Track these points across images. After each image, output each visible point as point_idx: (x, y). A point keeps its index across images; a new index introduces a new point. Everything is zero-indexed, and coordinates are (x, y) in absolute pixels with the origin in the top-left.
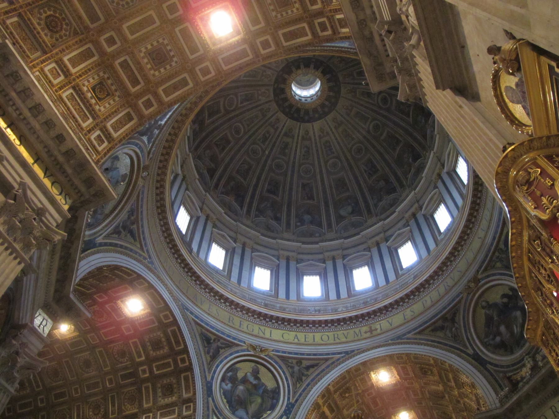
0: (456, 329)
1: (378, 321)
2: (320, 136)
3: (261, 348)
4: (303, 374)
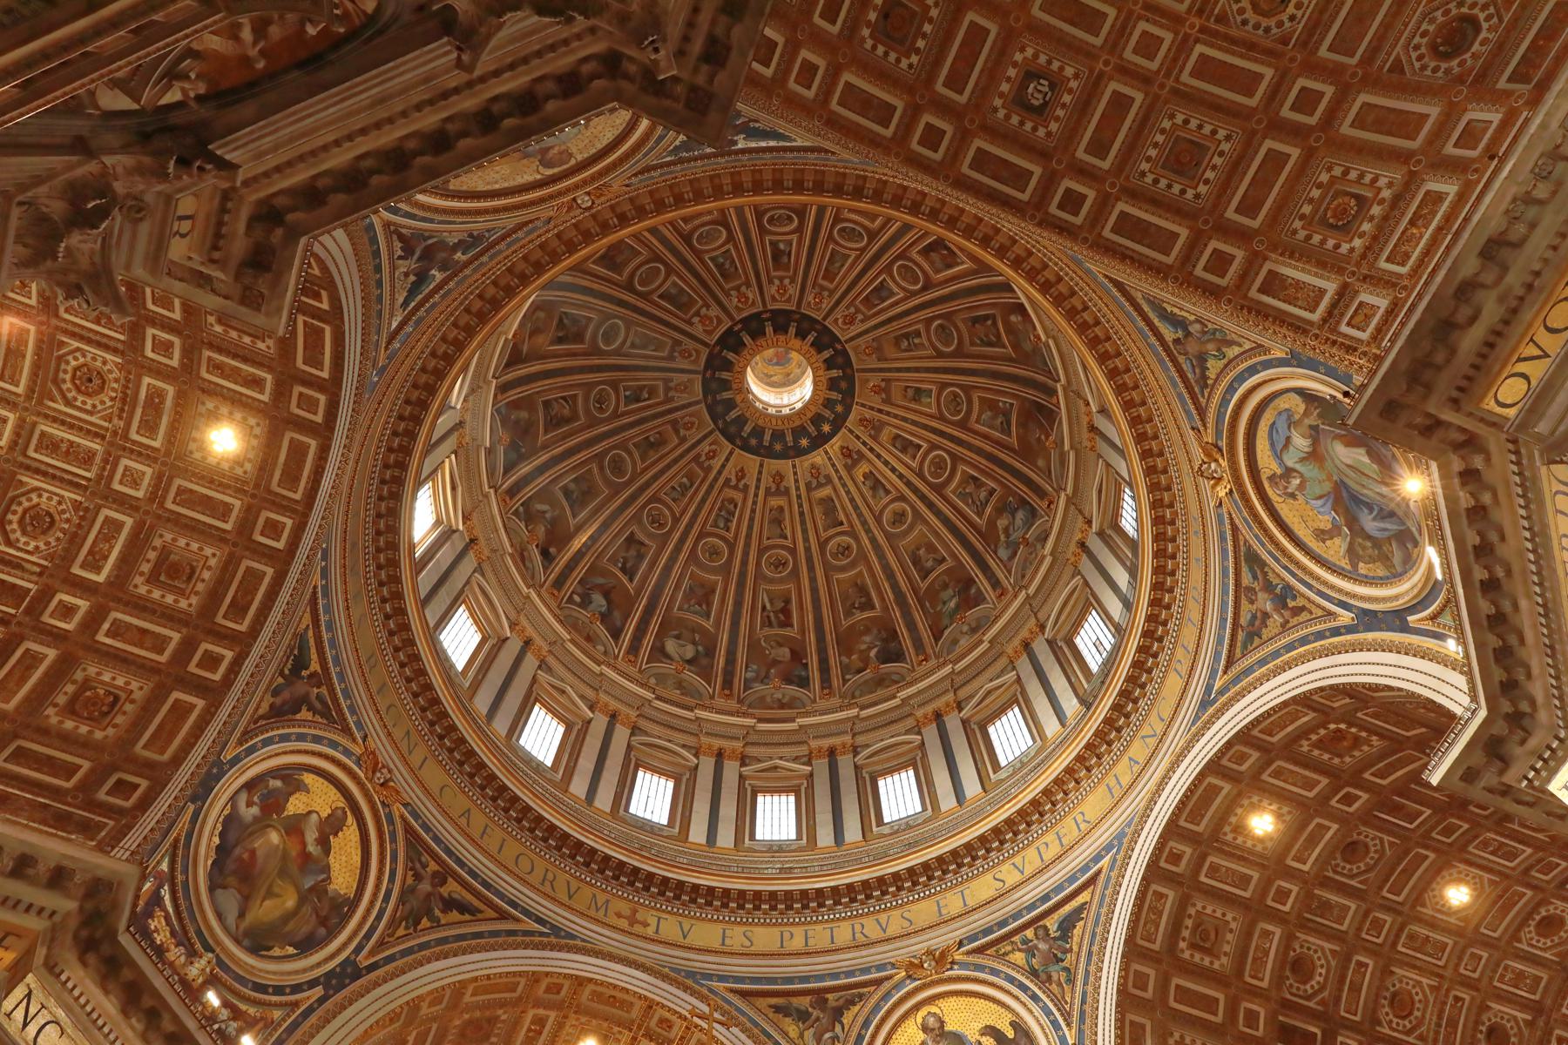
0: (835, 1038)
1: (658, 910)
2: (728, 481)
3: (391, 779)
4: (429, 913)
